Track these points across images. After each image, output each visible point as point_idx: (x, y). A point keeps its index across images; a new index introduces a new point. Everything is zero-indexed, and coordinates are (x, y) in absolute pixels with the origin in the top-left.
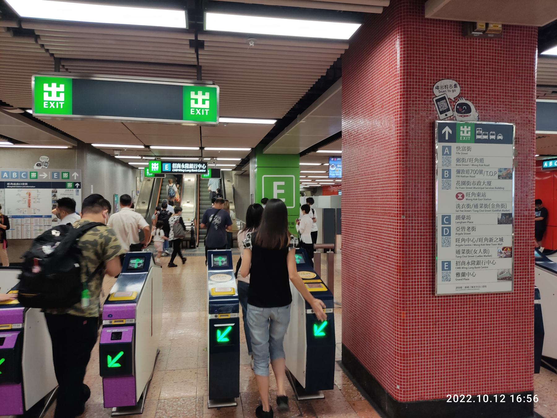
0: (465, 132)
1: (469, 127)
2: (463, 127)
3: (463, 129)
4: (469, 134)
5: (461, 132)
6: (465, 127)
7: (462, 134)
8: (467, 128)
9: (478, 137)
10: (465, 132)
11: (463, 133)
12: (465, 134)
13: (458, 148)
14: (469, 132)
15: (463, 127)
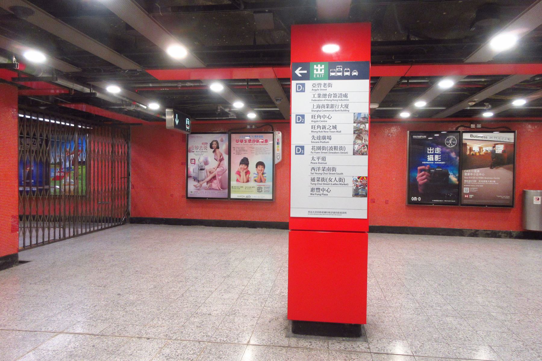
0: (319, 70)
1: (323, 66)
2: (317, 66)
3: (317, 68)
4: (323, 72)
5: (315, 71)
6: (319, 65)
7: (315, 72)
8: (321, 66)
9: (332, 74)
10: (319, 70)
11: (317, 70)
12: (319, 72)
13: (314, 85)
14: (323, 70)
15: (317, 66)
